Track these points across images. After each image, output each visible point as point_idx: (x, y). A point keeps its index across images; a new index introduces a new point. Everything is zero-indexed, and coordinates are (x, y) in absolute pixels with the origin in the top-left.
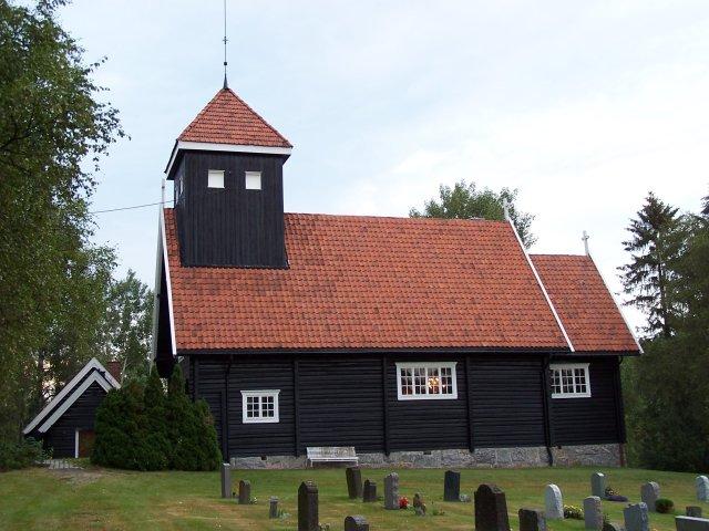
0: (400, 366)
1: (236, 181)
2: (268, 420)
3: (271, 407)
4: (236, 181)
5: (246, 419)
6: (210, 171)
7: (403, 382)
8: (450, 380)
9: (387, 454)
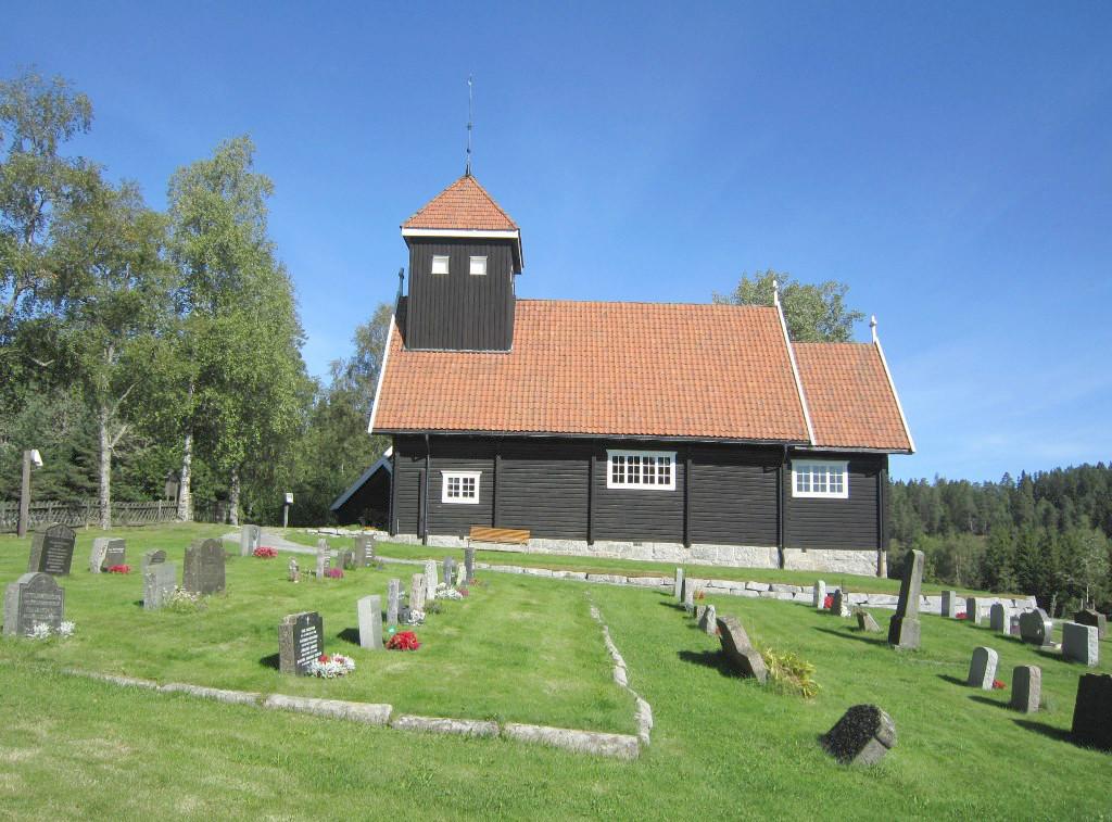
0: (611, 453)
1: (459, 267)
2: (468, 501)
3: (472, 488)
4: (459, 267)
5: (446, 499)
6: (435, 257)
7: (615, 469)
8: (668, 471)
9: (590, 543)
